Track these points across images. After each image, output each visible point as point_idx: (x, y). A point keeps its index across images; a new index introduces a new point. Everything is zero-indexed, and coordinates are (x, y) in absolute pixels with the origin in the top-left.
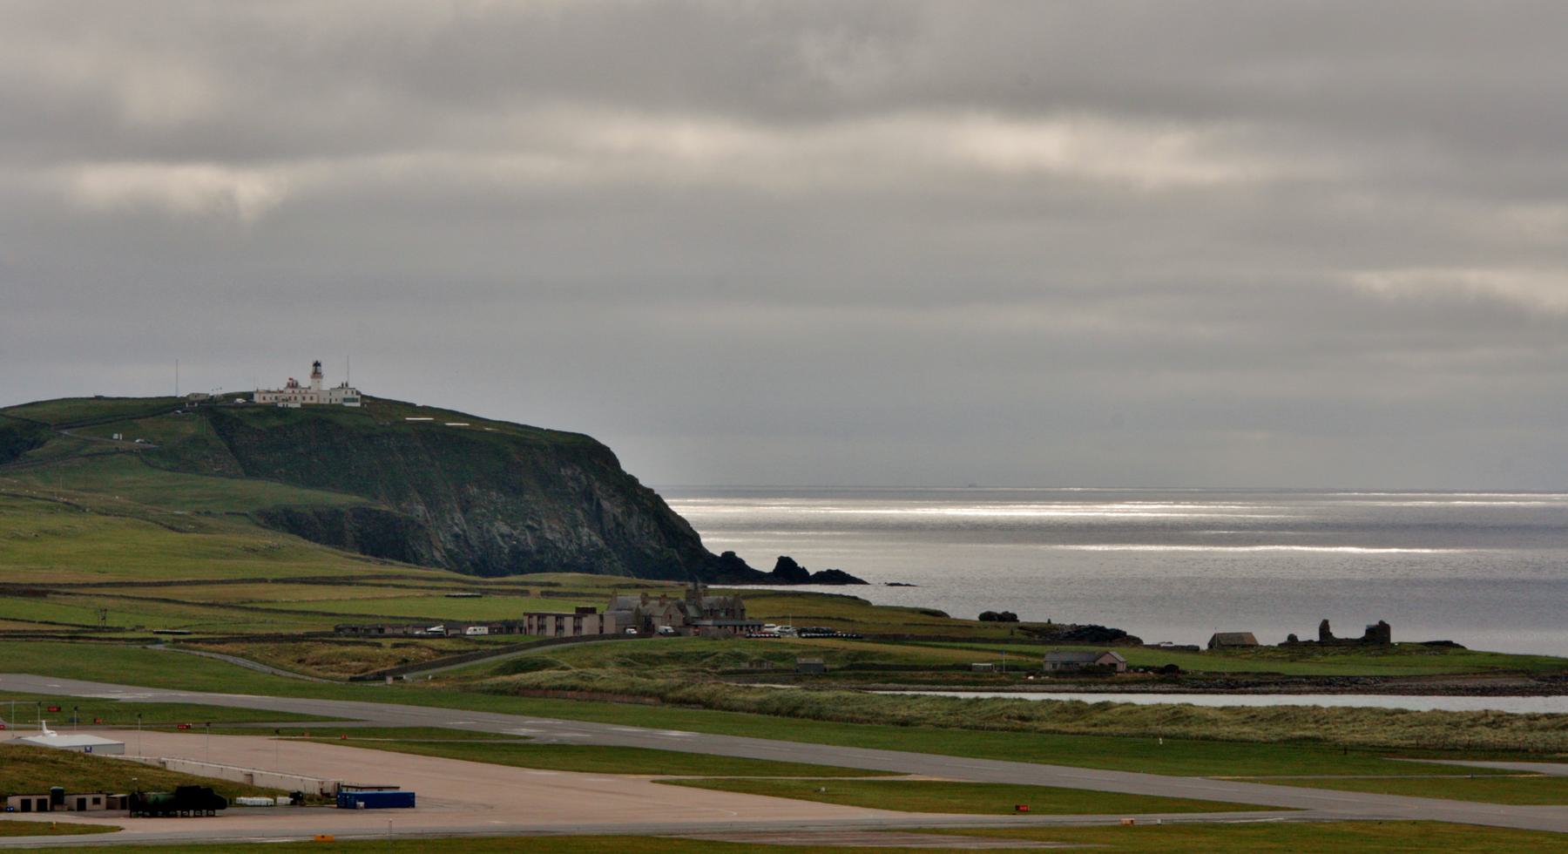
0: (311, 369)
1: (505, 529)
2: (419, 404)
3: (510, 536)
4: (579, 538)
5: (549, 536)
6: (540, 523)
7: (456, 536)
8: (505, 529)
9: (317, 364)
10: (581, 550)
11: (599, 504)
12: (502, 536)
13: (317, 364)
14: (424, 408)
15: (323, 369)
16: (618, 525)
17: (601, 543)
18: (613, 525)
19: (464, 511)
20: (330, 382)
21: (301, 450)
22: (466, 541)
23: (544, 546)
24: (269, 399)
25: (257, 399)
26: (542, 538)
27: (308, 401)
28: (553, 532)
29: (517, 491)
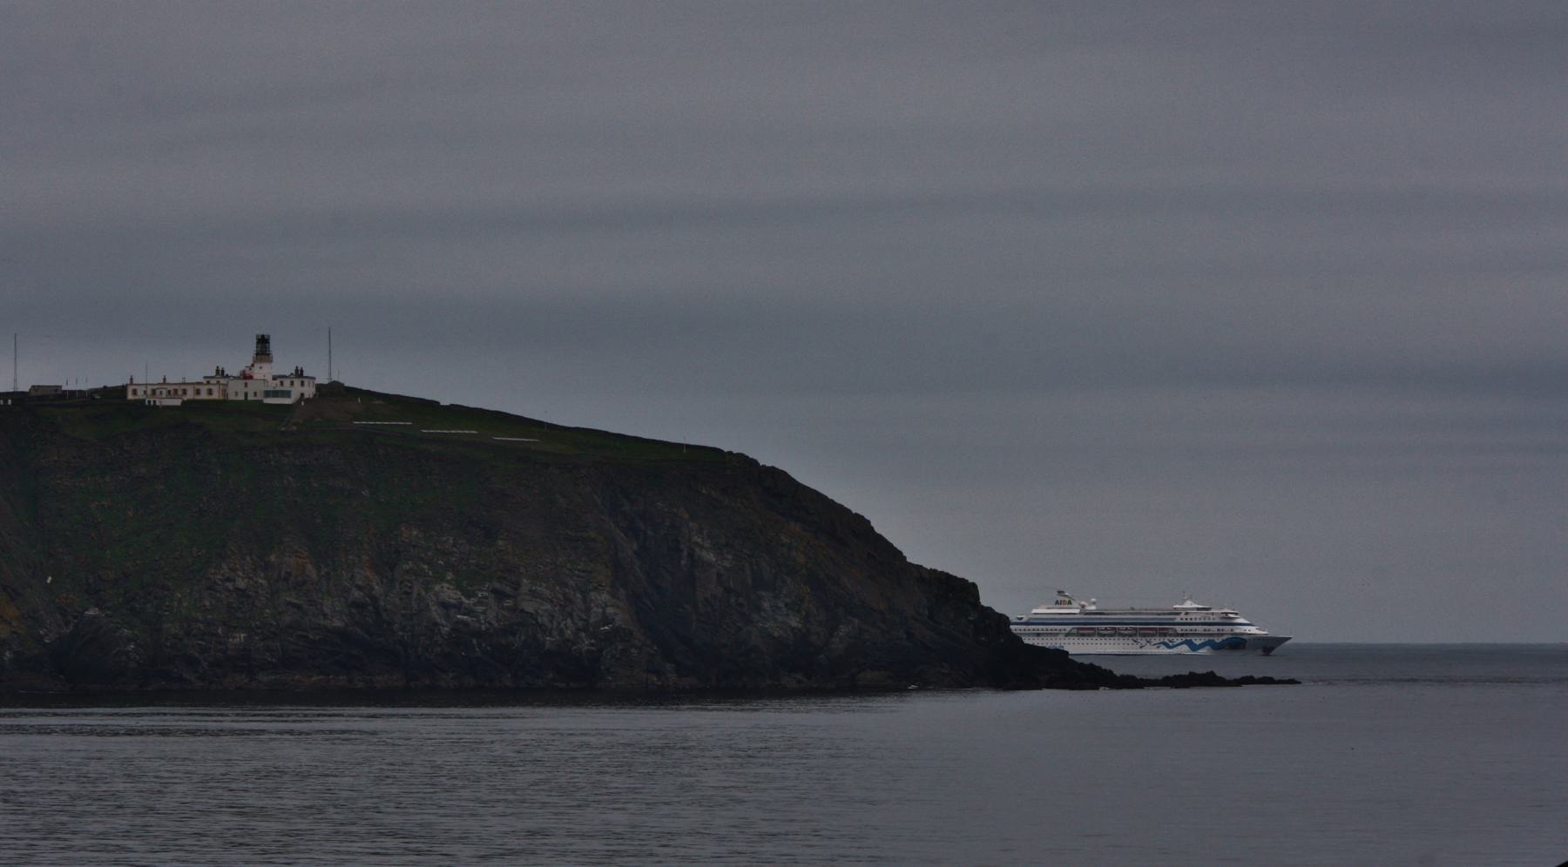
0: (252, 348)
1: (449, 593)
2: (445, 402)
3: (459, 607)
4: (588, 610)
5: (529, 607)
6: (517, 586)
8: (449, 593)
9: (263, 341)
11: (691, 555)
12: (445, 605)
13: (263, 341)
15: (274, 347)
17: (620, 616)
20: (282, 363)
25: (130, 397)
27: (204, 396)
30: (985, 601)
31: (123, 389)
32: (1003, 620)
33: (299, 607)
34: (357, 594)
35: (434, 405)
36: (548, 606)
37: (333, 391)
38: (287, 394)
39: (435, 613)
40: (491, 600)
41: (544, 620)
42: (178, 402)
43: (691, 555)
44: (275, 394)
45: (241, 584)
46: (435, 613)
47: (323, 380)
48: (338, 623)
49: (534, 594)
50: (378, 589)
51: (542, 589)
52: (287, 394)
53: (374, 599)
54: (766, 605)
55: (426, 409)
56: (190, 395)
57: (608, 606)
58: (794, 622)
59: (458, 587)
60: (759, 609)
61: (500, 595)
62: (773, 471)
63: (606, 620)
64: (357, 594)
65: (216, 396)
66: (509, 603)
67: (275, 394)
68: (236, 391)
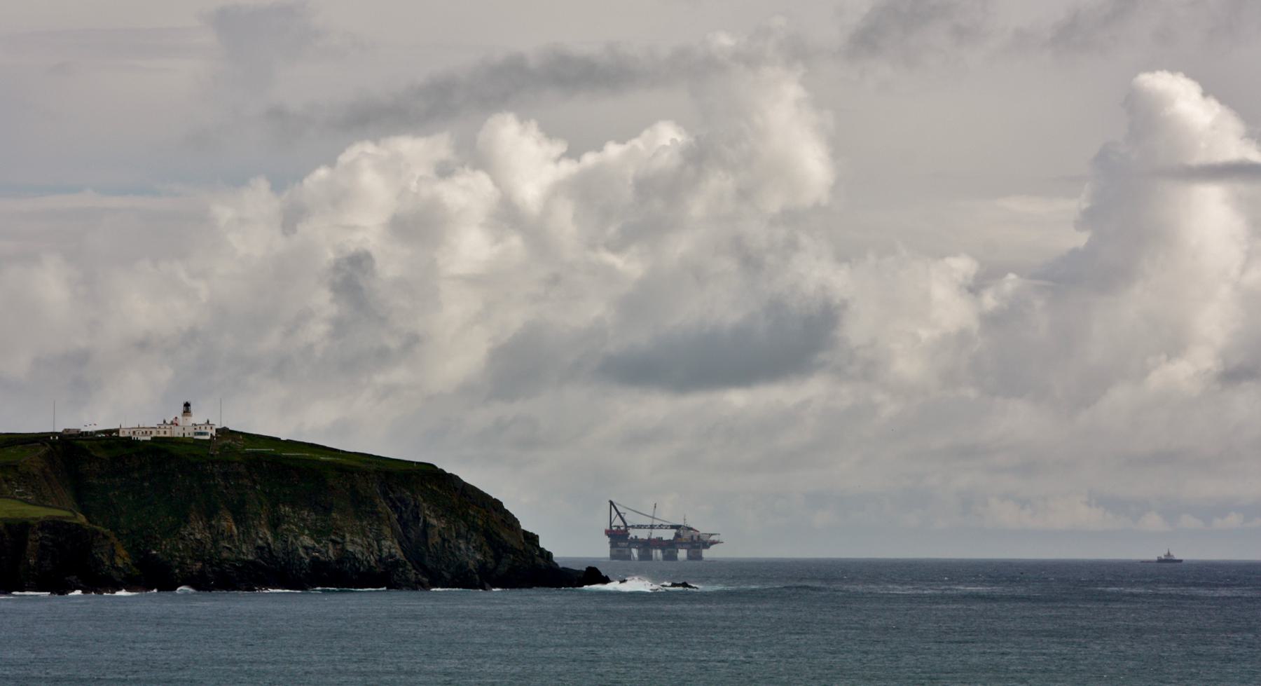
0: (182, 408)
1: (307, 541)
2: (283, 438)
3: (313, 549)
4: (380, 550)
5: (350, 548)
6: (343, 537)
7: (260, 548)
8: (307, 541)
9: (187, 405)
10: (380, 560)
11: (425, 521)
12: (305, 548)
13: (187, 405)
14: (288, 442)
15: (192, 408)
16: (444, 540)
17: (399, 554)
18: (439, 540)
19: (275, 524)
20: (197, 418)
21: (136, 475)
22: (270, 551)
23: (344, 556)
24: (127, 435)
26: (343, 550)
27: (162, 435)
28: (355, 546)
29: (327, 510)
30: (541, 545)
31: (117, 431)
32: (549, 555)
33: (229, 549)
34: (260, 542)
35: (277, 440)
36: (360, 548)
37: (224, 432)
38: (205, 434)
39: (301, 552)
40: (330, 545)
41: (359, 556)
42: (149, 438)
43: (425, 521)
44: (201, 434)
45: (198, 537)
46: (301, 552)
47: (218, 426)
48: (250, 558)
49: (353, 542)
50: (270, 540)
51: (357, 539)
52: (205, 434)
53: (269, 545)
54: (463, 546)
55: (276, 440)
56: (154, 434)
57: (391, 547)
58: (478, 557)
59: (312, 538)
60: (460, 549)
61: (335, 542)
62: (451, 475)
63: (391, 556)
64: (260, 542)
65: (168, 435)
66: (339, 547)
67: (201, 434)
68: (177, 433)
